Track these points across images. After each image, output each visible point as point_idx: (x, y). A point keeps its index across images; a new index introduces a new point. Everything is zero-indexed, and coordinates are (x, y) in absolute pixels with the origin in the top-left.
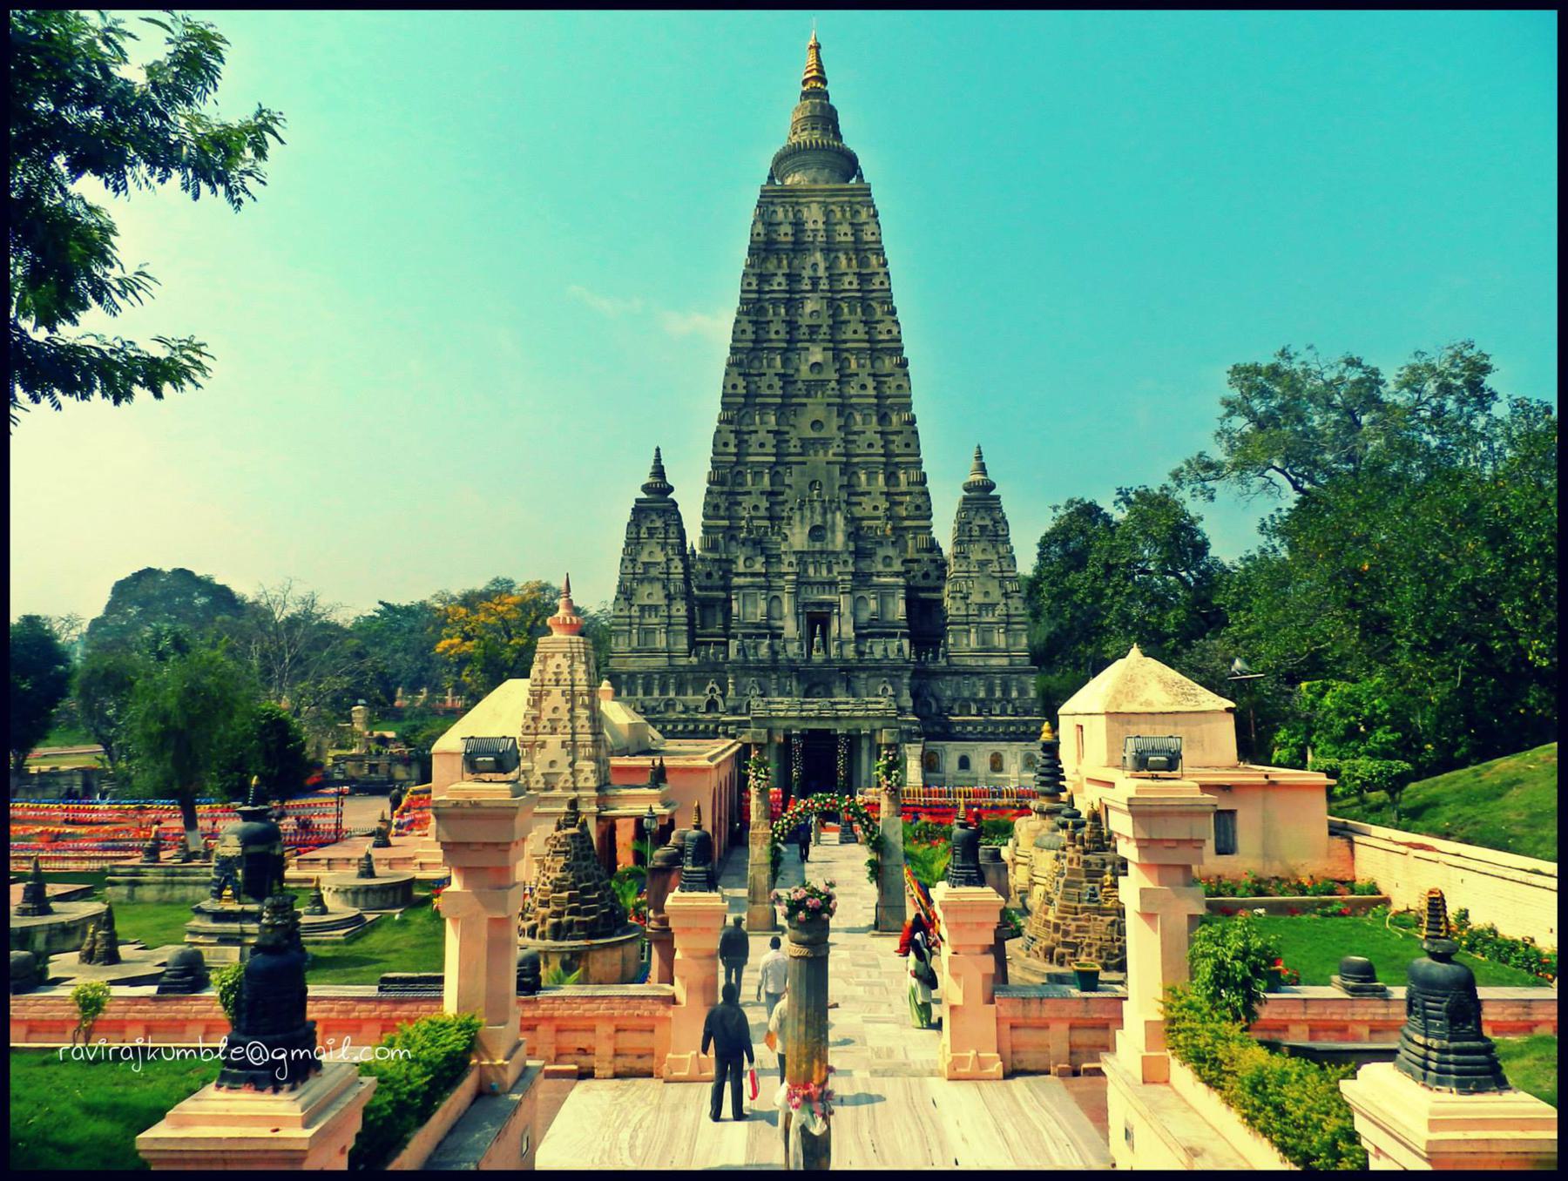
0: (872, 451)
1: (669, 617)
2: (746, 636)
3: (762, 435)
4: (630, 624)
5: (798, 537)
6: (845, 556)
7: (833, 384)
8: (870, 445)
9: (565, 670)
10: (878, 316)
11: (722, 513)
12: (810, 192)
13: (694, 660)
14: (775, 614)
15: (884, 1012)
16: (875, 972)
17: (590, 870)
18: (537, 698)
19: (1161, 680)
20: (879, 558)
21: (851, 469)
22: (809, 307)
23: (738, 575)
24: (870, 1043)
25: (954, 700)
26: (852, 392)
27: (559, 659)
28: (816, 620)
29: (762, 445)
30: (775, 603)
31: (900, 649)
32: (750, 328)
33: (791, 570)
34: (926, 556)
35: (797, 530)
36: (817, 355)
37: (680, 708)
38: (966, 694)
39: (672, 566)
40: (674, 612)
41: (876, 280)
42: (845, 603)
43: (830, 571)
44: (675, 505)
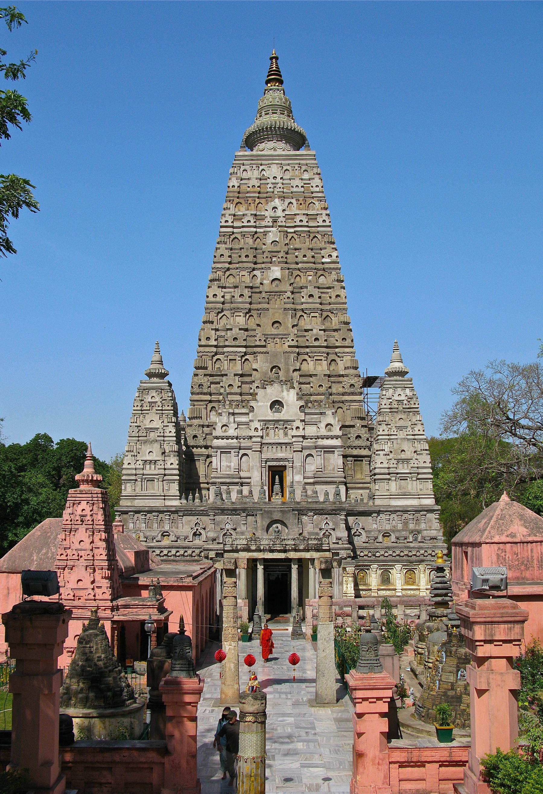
0: (317, 343)
1: (165, 469)
3: (236, 331)
4: (136, 475)
5: (262, 408)
6: (298, 423)
7: (289, 294)
8: (317, 339)
9: (88, 512)
10: (322, 245)
11: (205, 391)
12: (271, 157)
13: (184, 501)
14: (244, 466)
15: (316, 760)
19: (522, 517)
20: (322, 425)
21: (301, 357)
22: (271, 237)
23: (217, 438)
24: (304, 780)
25: (379, 531)
26: (303, 300)
27: (84, 504)
28: (276, 473)
29: (235, 339)
30: (244, 458)
31: (338, 494)
32: (227, 253)
33: (256, 434)
34: (359, 423)
35: (260, 404)
36: (276, 272)
37: (172, 538)
38: (388, 527)
39: (167, 430)
40: (168, 466)
41: (320, 220)
42: (298, 458)
43: (286, 434)
44: (170, 385)
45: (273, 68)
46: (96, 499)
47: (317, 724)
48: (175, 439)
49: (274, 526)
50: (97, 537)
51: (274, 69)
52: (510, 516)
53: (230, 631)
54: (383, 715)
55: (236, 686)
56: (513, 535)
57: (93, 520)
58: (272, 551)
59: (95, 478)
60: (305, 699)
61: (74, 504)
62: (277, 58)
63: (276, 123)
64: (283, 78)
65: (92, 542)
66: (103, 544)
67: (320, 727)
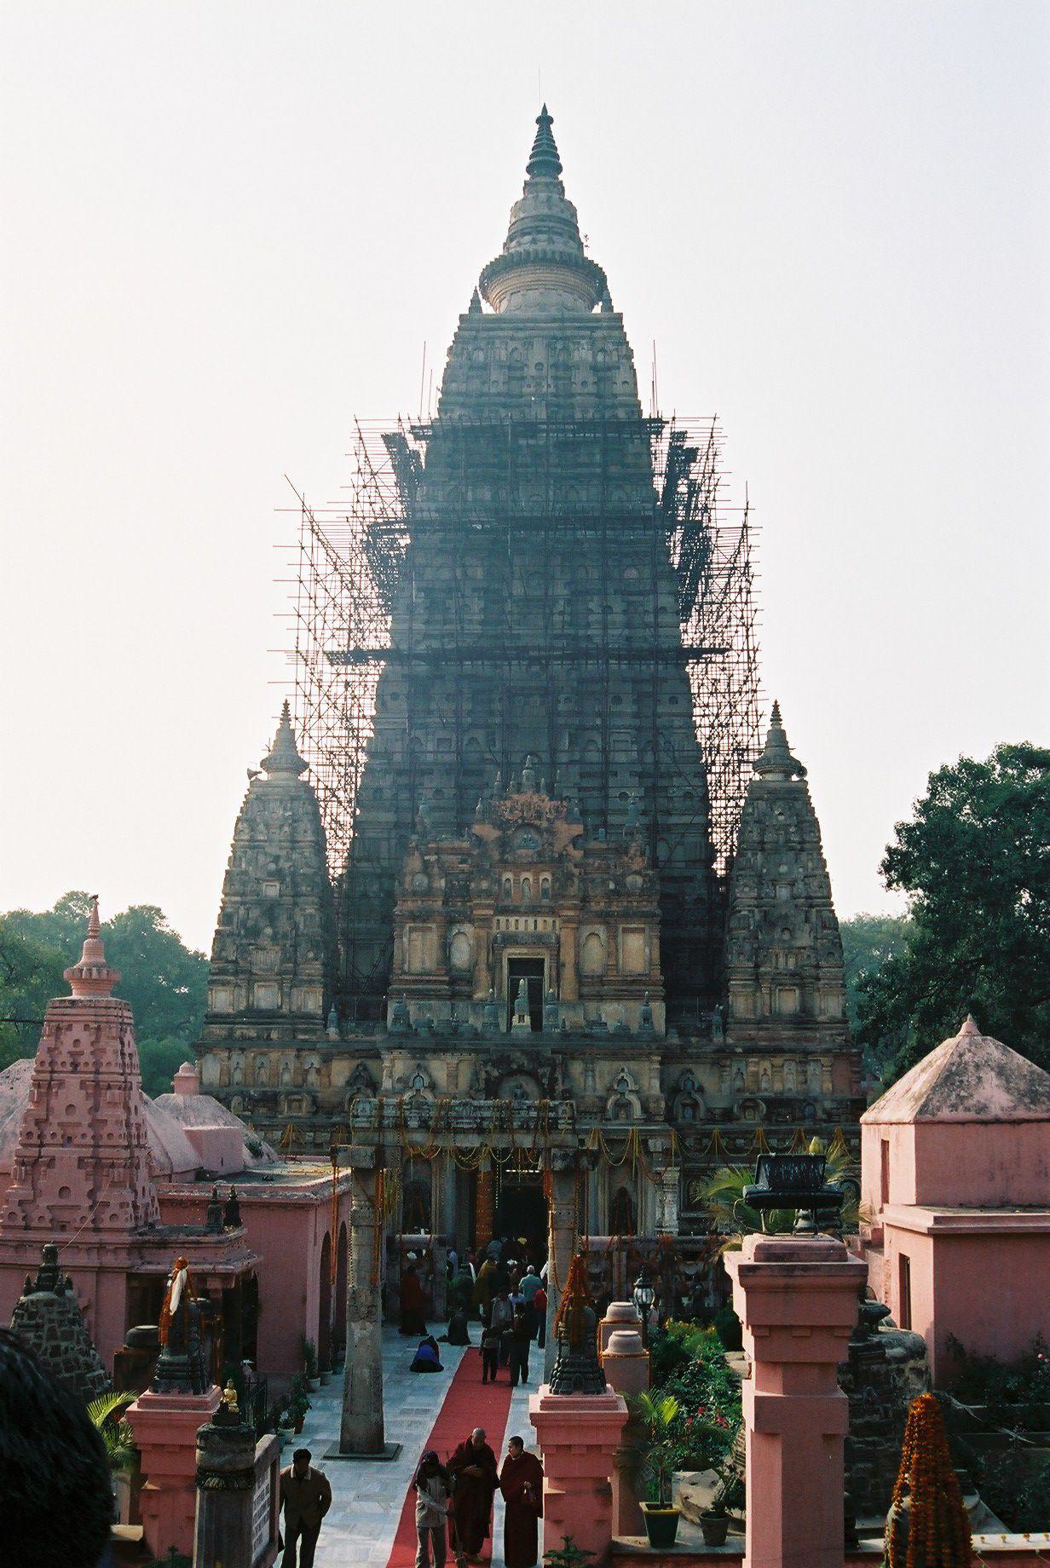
2: (414, 994)
17: (71, 1355)
18: (45, 1088)
19: (1001, 1071)
52: (977, 1066)
56: (983, 1108)
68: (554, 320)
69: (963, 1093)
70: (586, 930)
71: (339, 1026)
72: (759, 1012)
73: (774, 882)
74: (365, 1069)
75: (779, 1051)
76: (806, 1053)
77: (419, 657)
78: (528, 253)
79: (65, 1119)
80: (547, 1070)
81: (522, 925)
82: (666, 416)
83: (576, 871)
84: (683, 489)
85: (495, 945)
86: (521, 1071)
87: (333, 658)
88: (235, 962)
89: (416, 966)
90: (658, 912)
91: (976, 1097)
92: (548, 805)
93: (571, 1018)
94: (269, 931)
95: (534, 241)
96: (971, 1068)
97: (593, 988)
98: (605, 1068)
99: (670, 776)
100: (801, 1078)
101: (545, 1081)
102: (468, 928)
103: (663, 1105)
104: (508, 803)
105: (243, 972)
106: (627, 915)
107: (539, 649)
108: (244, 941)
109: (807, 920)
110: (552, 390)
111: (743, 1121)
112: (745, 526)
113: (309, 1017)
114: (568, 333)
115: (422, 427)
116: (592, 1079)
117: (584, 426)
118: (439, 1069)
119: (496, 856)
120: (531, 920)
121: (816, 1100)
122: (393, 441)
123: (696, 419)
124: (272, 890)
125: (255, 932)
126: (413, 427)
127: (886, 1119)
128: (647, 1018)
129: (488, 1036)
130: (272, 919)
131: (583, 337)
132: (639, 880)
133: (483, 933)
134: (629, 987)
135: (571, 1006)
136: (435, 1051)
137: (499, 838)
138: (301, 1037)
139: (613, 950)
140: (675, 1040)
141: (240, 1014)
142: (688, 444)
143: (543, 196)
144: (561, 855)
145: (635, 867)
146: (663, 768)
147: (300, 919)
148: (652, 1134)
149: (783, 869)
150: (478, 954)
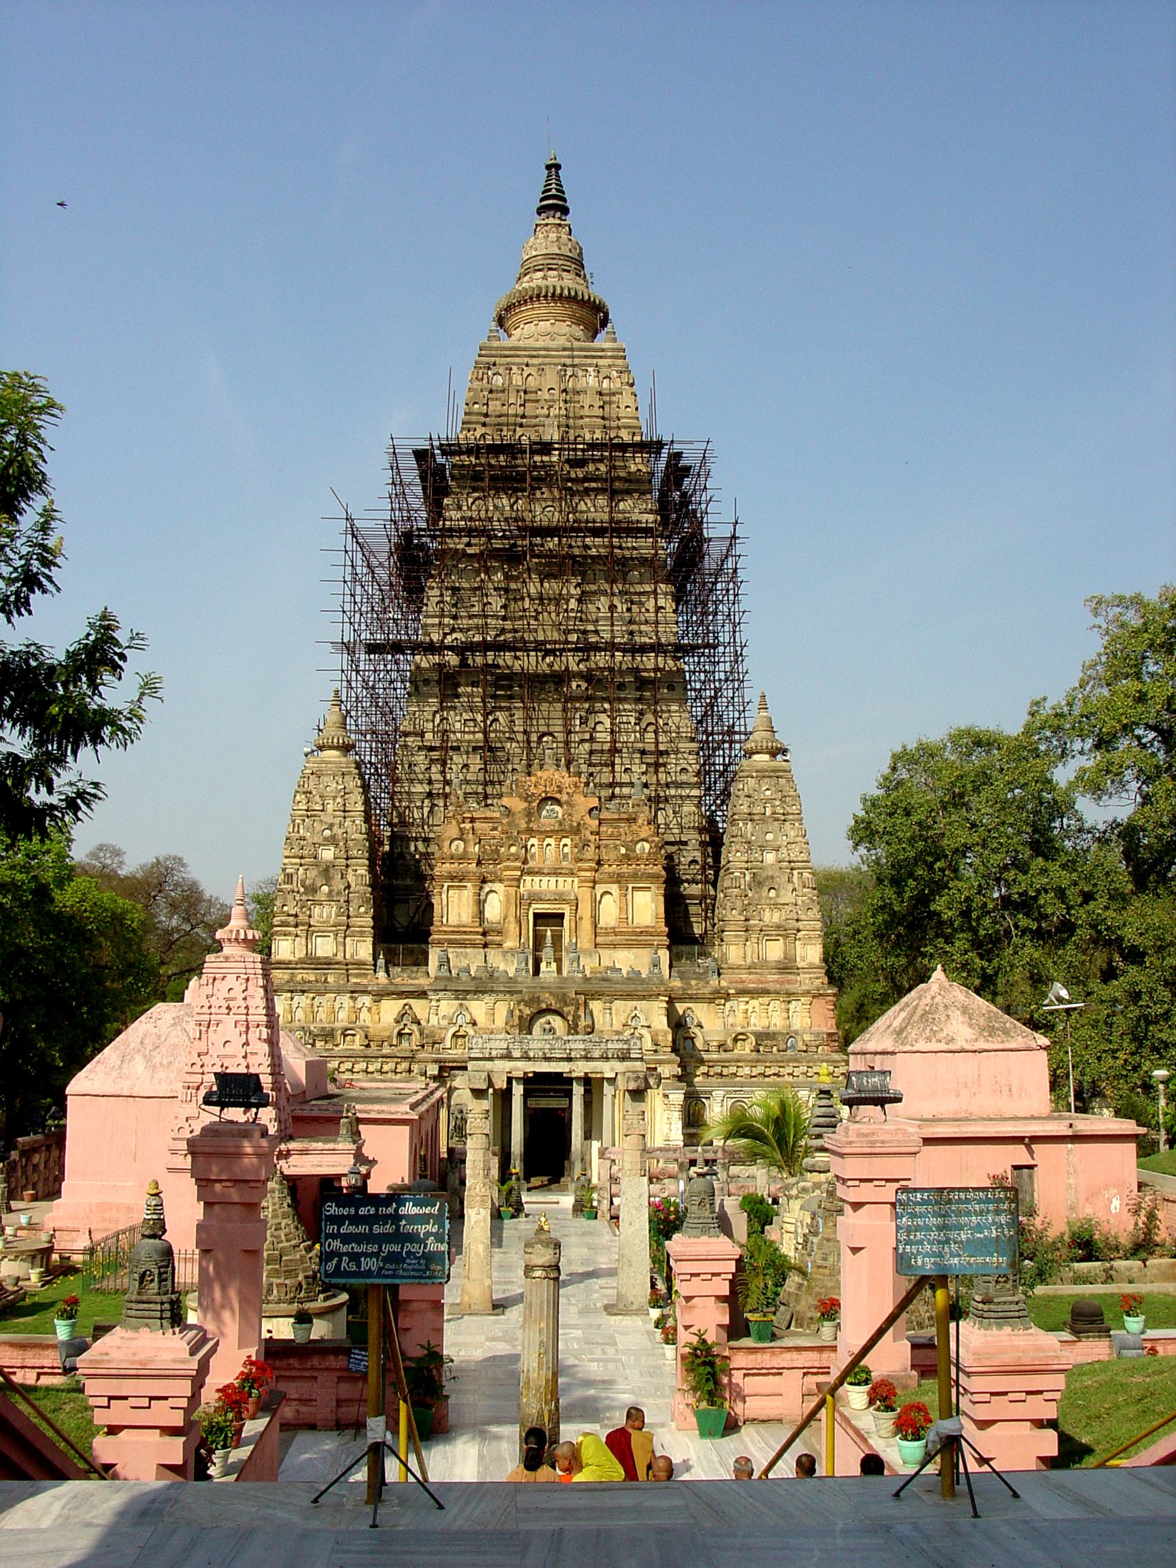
7: (573, 604)
16: (611, 1351)
19: (965, 1010)
45: (550, 190)
46: (253, 971)
47: (618, 1338)
48: (367, 862)
49: (543, 1020)
50: (254, 1034)
51: (554, 192)
52: (946, 1007)
53: (477, 1191)
54: (720, 1298)
55: (487, 1282)
56: (951, 1040)
57: (247, 1007)
58: (547, 1059)
59: (250, 937)
60: (599, 1305)
61: (215, 979)
62: (558, 167)
63: (554, 287)
64: (568, 204)
65: (247, 1043)
66: (266, 1048)
67: (623, 1342)
68: (564, 349)
69: (935, 1028)
70: (600, 888)
71: (387, 971)
72: (749, 960)
73: (762, 848)
74: (411, 1008)
75: (765, 992)
76: (789, 994)
77: (451, 648)
78: (540, 288)
79: (223, 1052)
80: (572, 1009)
81: (546, 884)
82: (666, 438)
83: (592, 838)
84: (676, 495)
85: (522, 902)
86: (549, 1011)
87: (372, 648)
88: (296, 916)
89: (453, 920)
90: (663, 873)
91: (945, 1032)
92: (567, 781)
93: (589, 964)
94: (325, 889)
95: (545, 278)
96: (941, 1008)
97: (603, 938)
98: (622, 1008)
99: (667, 753)
100: (785, 1015)
101: (570, 1018)
102: (498, 886)
103: (670, 1038)
104: (533, 779)
105: (303, 925)
106: (635, 876)
107: (555, 642)
108: (304, 898)
109: (790, 881)
110: (563, 412)
111: (736, 1051)
112: (734, 537)
113: (360, 964)
114: (576, 361)
115: (449, 445)
116: (609, 1016)
117: (592, 446)
118: (478, 1008)
119: (523, 825)
120: (553, 879)
121: (796, 1033)
122: (421, 456)
123: (692, 442)
124: (327, 854)
125: (312, 890)
126: (441, 445)
127: (872, 1050)
128: (656, 964)
129: (520, 979)
130: (328, 881)
131: (590, 365)
132: (647, 846)
133: (512, 890)
134: (636, 938)
135: (589, 953)
136: (475, 992)
137: (525, 809)
138: (355, 980)
139: (625, 907)
140: (677, 983)
141: (301, 961)
142: (683, 463)
143: (553, 236)
144: (579, 824)
145: (643, 836)
146: (662, 747)
147: (351, 878)
148: (661, 1062)
149: (770, 837)
150: (508, 910)
